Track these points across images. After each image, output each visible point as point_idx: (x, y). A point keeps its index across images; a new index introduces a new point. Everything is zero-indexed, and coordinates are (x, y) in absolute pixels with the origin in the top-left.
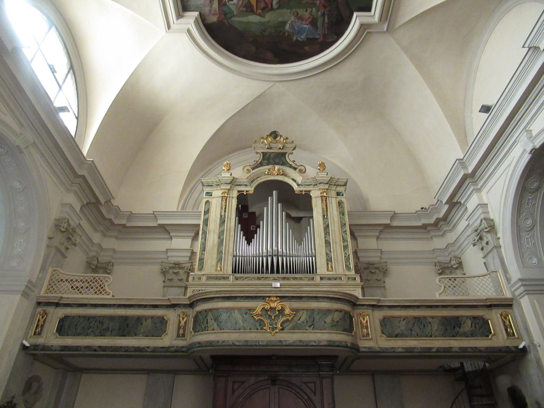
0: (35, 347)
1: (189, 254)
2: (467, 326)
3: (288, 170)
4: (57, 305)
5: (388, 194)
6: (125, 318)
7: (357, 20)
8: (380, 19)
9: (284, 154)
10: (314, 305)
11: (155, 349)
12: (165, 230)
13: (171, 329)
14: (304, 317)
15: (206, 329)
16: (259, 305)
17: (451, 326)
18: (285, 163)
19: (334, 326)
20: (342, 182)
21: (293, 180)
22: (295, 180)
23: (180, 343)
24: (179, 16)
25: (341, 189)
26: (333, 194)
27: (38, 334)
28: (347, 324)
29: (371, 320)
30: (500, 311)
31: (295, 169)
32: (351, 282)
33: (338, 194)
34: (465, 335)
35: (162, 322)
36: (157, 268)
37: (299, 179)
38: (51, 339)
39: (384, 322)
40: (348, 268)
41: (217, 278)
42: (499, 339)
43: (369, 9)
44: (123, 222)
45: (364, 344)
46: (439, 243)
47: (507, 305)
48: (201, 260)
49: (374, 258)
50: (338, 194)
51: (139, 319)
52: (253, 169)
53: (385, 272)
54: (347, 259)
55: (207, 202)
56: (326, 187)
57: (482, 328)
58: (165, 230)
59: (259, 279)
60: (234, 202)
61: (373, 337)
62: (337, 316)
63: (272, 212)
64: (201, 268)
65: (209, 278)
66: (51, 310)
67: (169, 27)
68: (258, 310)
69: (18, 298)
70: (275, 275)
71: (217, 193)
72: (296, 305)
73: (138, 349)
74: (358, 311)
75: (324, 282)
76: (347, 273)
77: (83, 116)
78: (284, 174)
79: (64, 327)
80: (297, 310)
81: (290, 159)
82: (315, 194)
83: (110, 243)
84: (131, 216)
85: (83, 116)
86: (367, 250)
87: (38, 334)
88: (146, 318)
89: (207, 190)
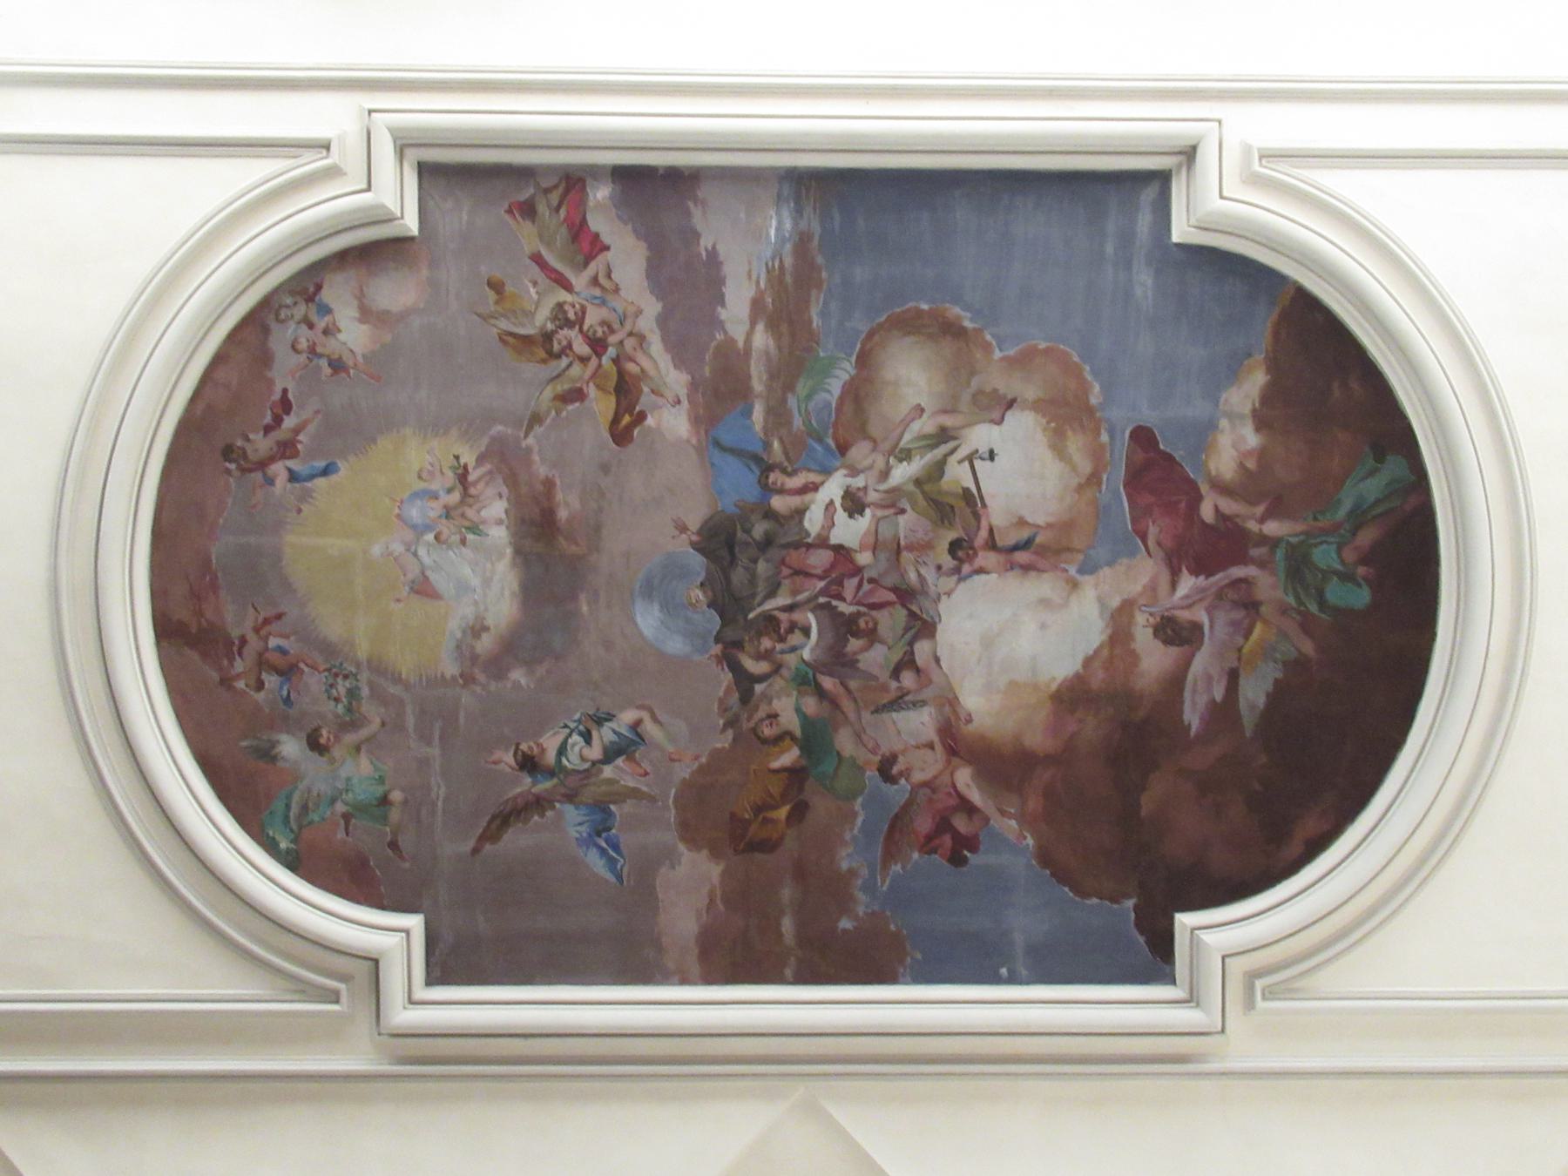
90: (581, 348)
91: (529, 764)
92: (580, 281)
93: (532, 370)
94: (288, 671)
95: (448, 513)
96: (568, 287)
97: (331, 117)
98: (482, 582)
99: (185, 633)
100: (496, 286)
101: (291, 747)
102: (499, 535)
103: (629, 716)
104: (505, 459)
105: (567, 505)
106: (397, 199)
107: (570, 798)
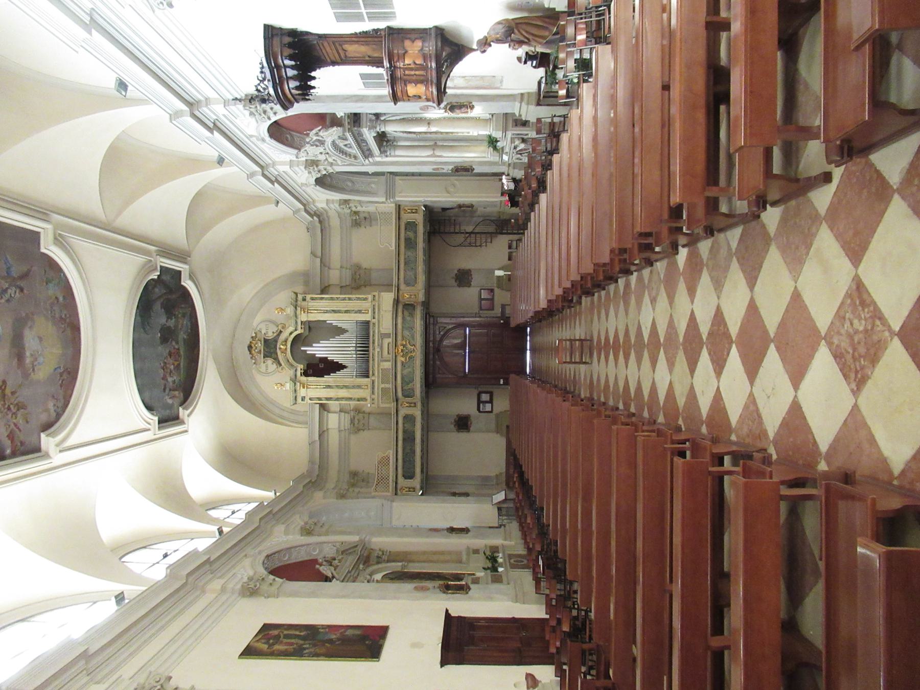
0: (422, 488)
1: (343, 414)
2: (411, 234)
3: (283, 337)
4: (396, 483)
5: (295, 256)
6: (404, 440)
7: (49, 248)
8: (186, 263)
9: (266, 341)
10: (400, 326)
11: (423, 419)
12: (323, 433)
13: (410, 411)
14: (407, 333)
15: (413, 390)
16: (400, 359)
17: (410, 244)
18: (275, 340)
19: (412, 315)
20: (294, 296)
21: (291, 334)
22: (290, 332)
23: (419, 405)
24: (183, 423)
25: (300, 297)
26: (304, 303)
27: (414, 489)
28: (409, 307)
29: (407, 295)
30: (402, 212)
31: (281, 332)
32: (377, 298)
33: (304, 300)
34: (416, 237)
35: (406, 417)
36: (353, 437)
37: (292, 329)
38: (416, 482)
39: (407, 284)
40: (366, 299)
41: (373, 388)
42: (419, 218)
43: (180, 272)
44: (317, 466)
45: (421, 297)
46: (335, 222)
47: (399, 207)
48: (358, 400)
49: (348, 274)
50: (304, 300)
51: (404, 432)
52: (281, 365)
53: (358, 267)
54: (359, 299)
55: (311, 399)
56: (299, 309)
57: (411, 226)
58: (323, 433)
59: (373, 360)
60: (310, 379)
61: (416, 292)
62: (406, 313)
63: (320, 350)
64: (365, 399)
65: (373, 393)
66: (399, 487)
67: (186, 431)
68: (403, 359)
69: (394, 504)
70: (371, 349)
71: (302, 392)
72: (399, 338)
73: (422, 429)
74: (400, 298)
75: (376, 317)
76: (370, 300)
77: (248, 500)
78: (286, 341)
79: (409, 475)
80: (403, 337)
81: (270, 336)
82: (304, 317)
83: (333, 474)
84: (311, 462)
85: (248, 500)
86: (341, 278)
87: (414, 489)
88: (404, 427)
89: (299, 400)
90: (12, 406)
91: (22, 290)
92: (12, 426)
93: (21, 399)
94: (61, 318)
95: (36, 359)
96: (15, 425)
97: (58, 458)
98: (31, 341)
99: (76, 328)
100: (27, 422)
101: (61, 299)
102: (28, 354)
103: (3, 301)
104: (26, 375)
105: (15, 361)
106: (47, 442)
107: (14, 278)
